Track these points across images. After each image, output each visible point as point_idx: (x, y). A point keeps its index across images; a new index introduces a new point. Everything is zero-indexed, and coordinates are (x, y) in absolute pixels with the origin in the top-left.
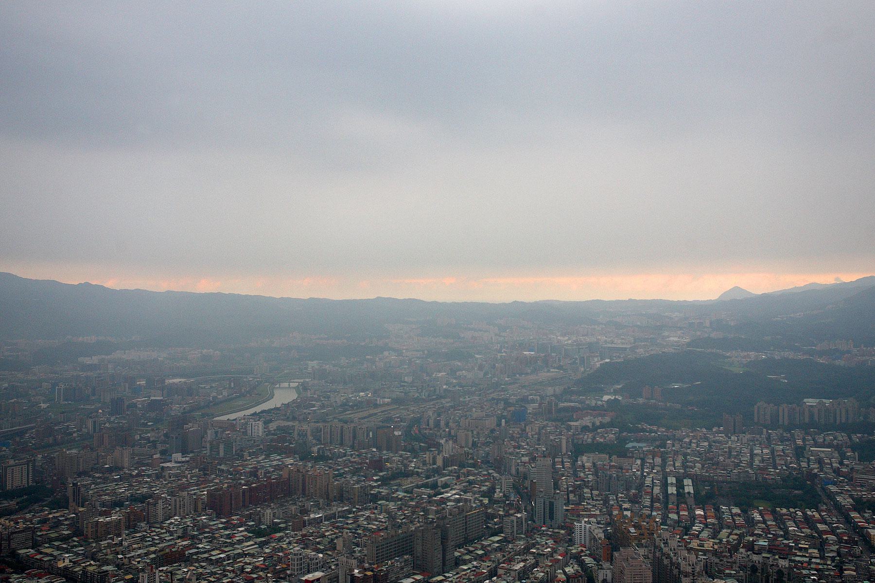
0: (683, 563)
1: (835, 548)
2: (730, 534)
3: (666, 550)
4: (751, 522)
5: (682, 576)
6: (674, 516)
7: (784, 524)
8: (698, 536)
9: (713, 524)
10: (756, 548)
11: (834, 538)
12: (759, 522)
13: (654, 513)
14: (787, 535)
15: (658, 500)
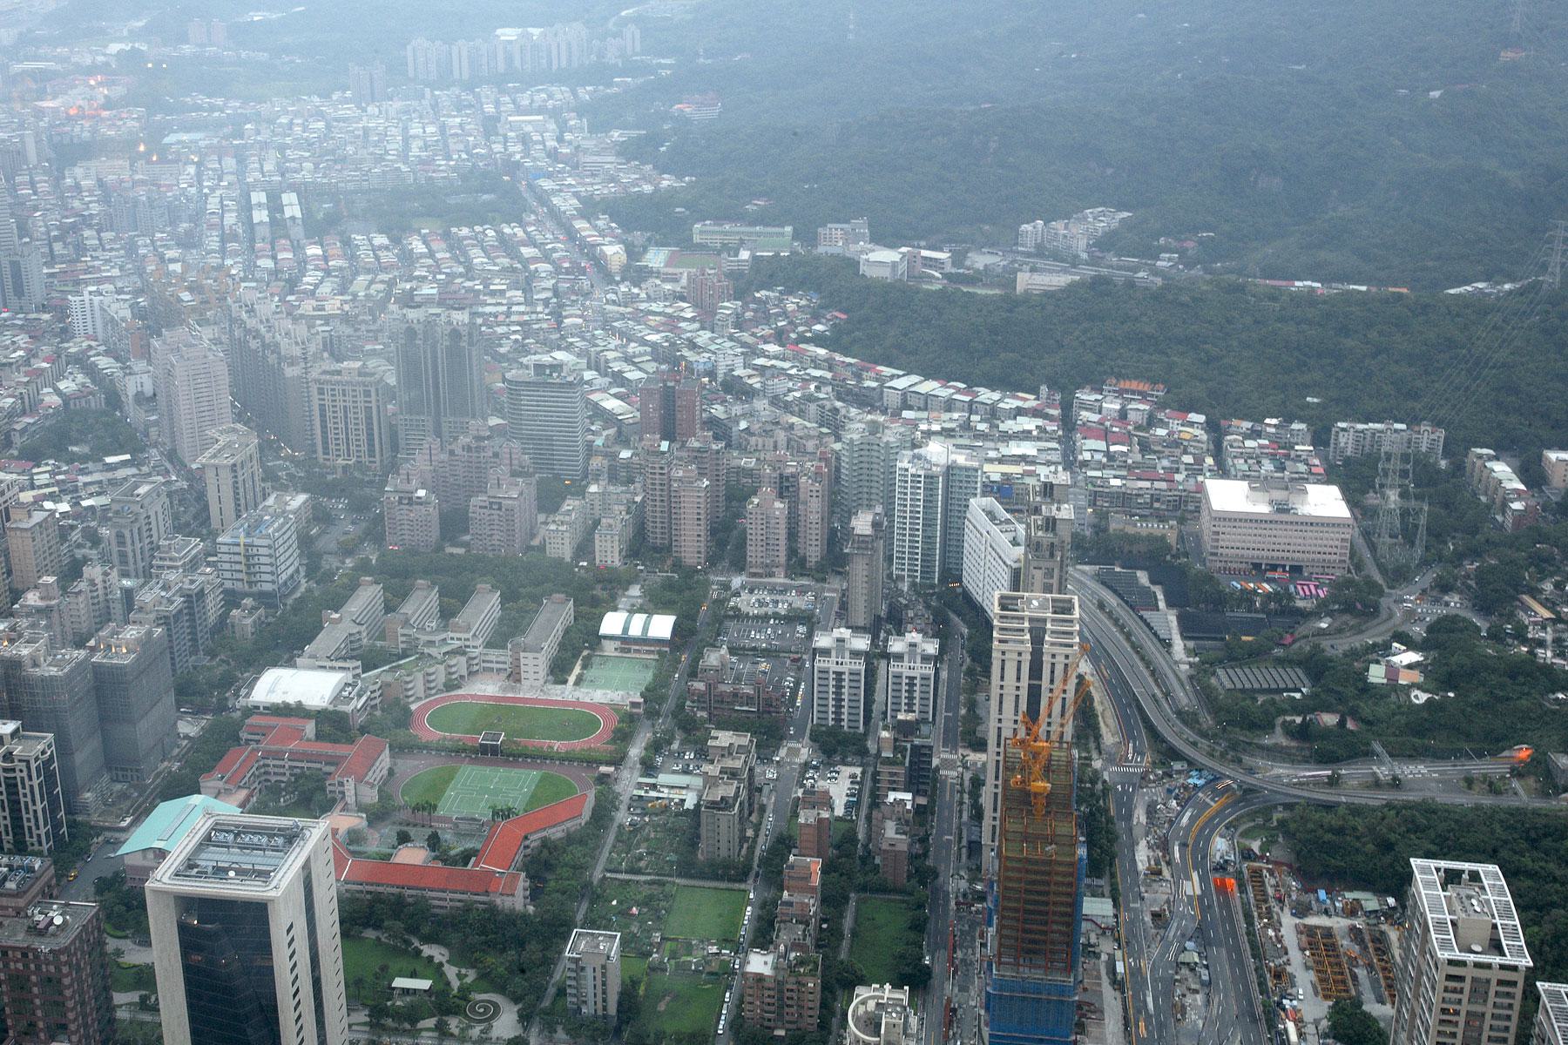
0: (284, 343)
1: (550, 283)
2: (372, 282)
3: (251, 323)
4: (408, 258)
5: (284, 366)
6: (266, 263)
7: (465, 253)
8: (313, 293)
9: (341, 269)
10: (417, 299)
11: (548, 267)
12: (422, 256)
13: (229, 262)
14: (469, 273)
15: (234, 237)
